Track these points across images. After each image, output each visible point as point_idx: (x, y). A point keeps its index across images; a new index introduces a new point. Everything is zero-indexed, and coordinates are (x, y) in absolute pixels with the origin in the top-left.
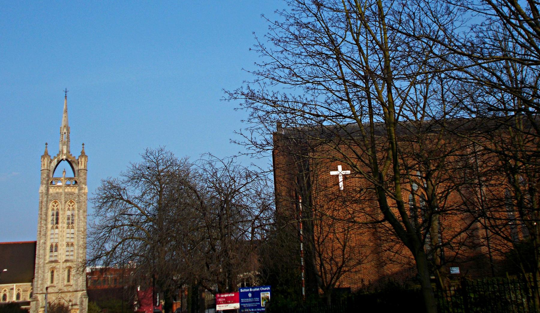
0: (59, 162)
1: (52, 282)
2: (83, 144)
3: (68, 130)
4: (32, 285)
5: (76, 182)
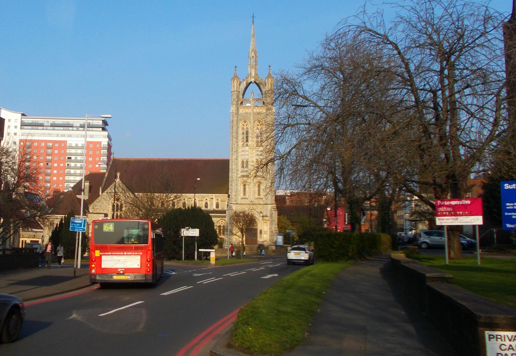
0: (248, 85)
1: (245, 195)
2: (270, 66)
3: (255, 54)
4: (229, 196)
5: (264, 103)
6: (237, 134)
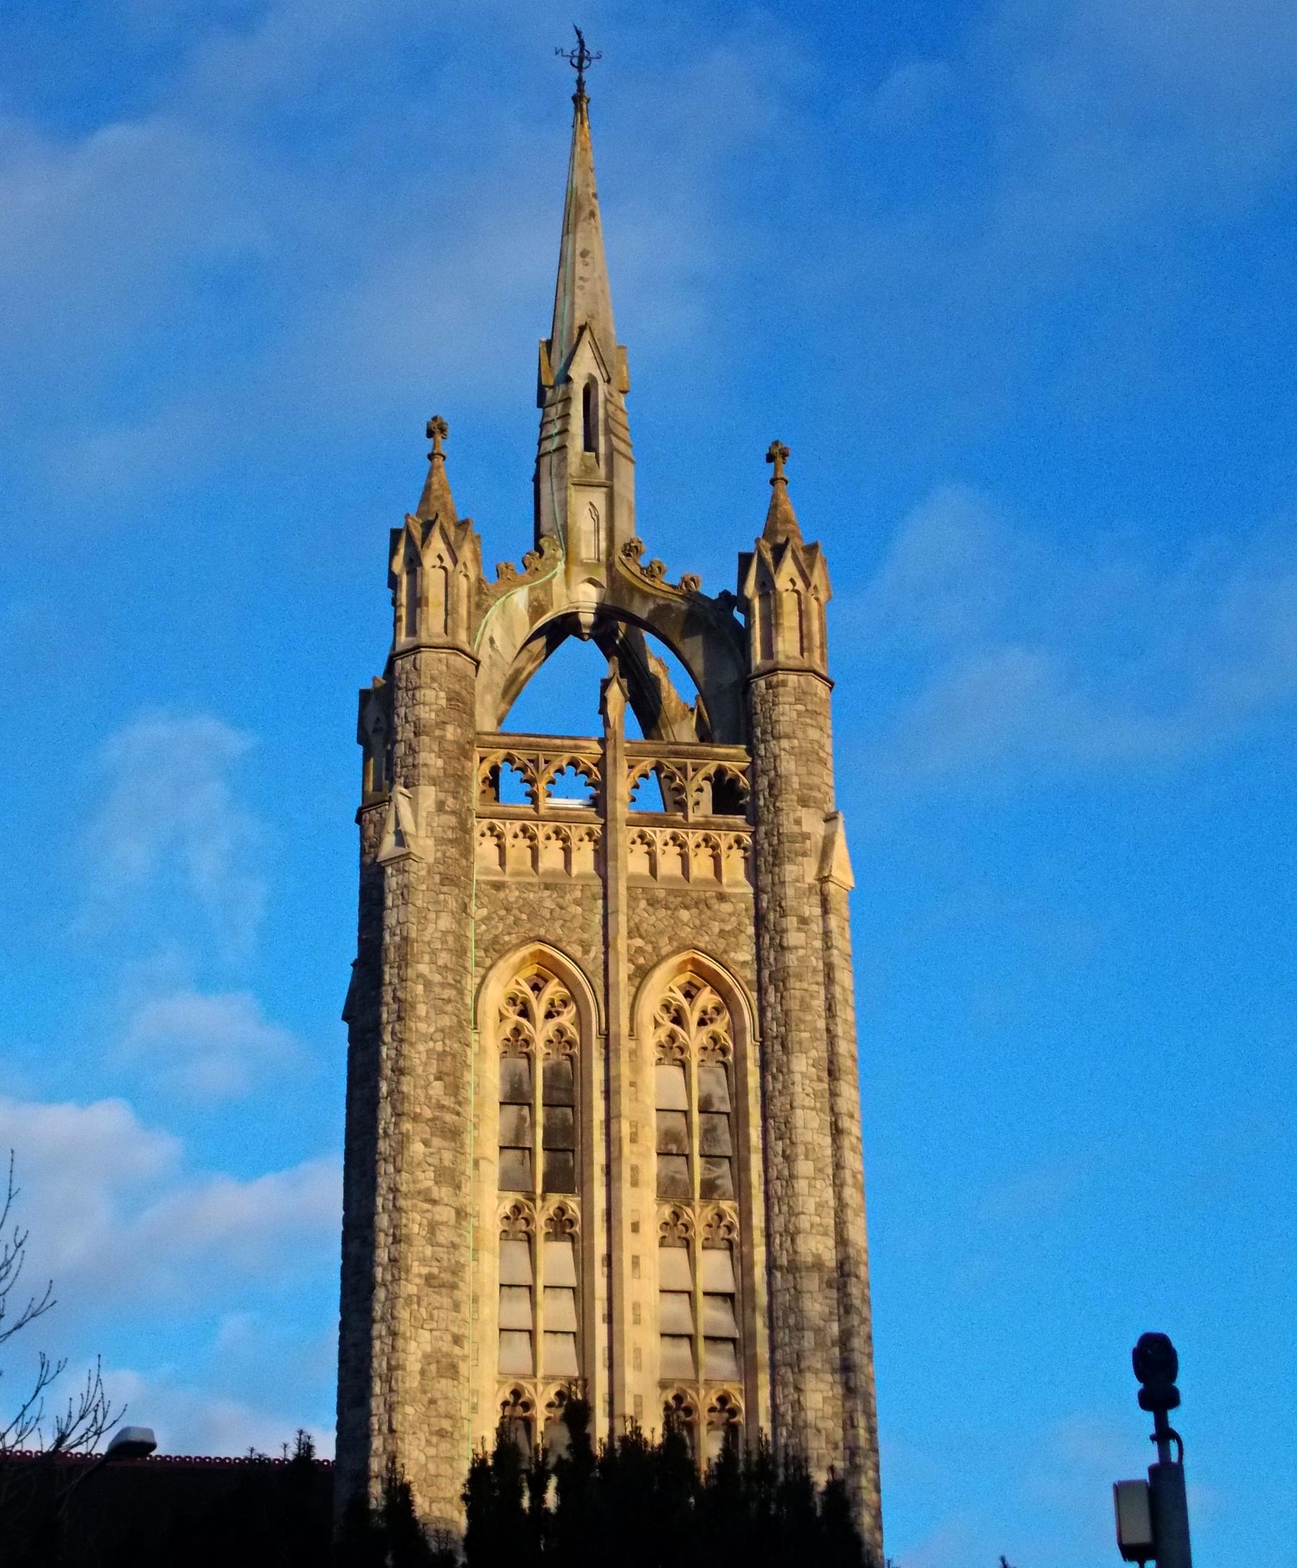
6: (455, 1088)
